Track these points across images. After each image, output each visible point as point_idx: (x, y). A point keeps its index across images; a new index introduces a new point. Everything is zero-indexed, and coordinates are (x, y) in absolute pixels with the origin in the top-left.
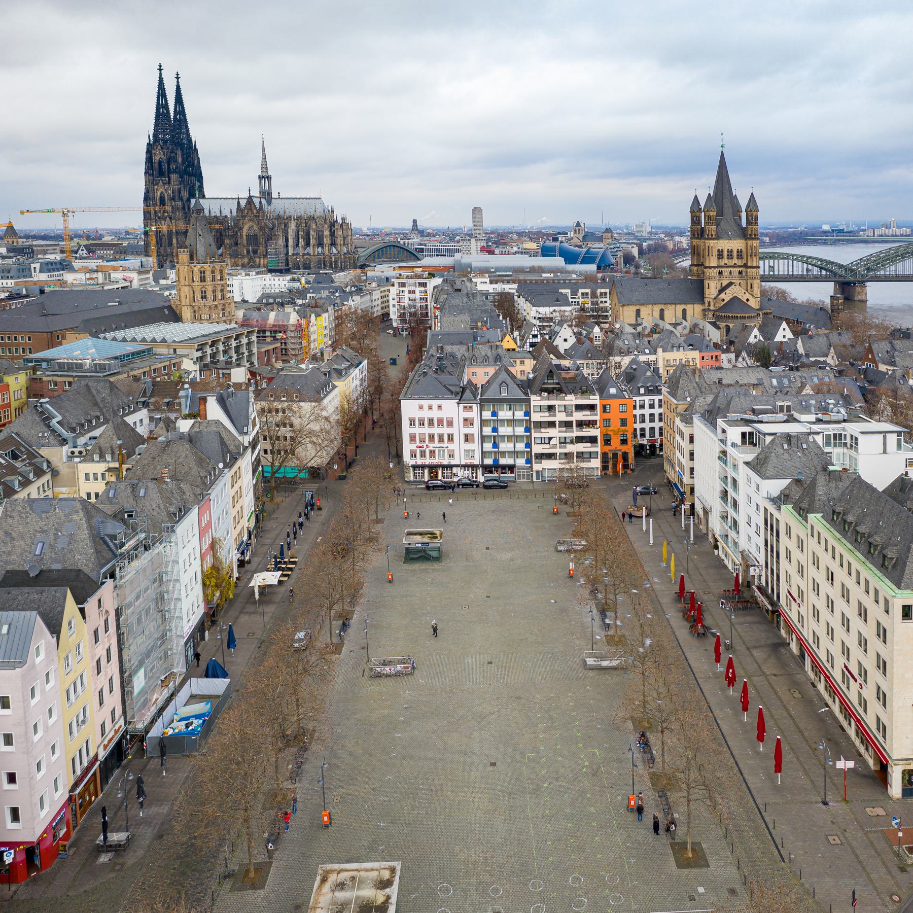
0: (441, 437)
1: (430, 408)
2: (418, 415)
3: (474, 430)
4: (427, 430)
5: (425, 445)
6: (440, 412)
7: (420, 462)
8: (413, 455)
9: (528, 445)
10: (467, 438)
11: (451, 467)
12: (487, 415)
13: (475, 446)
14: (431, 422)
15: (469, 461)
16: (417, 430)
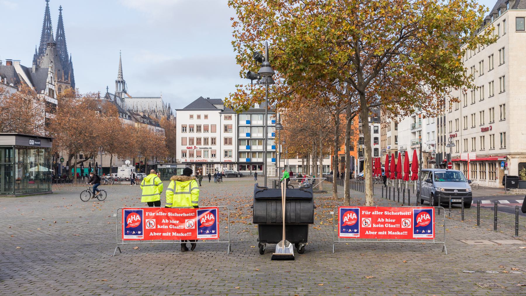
0: (206, 140)
1: (199, 117)
2: (189, 122)
3: (232, 135)
4: (195, 135)
6: (206, 120)
7: (189, 160)
8: (184, 154)
11: (213, 163)
13: (233, 148)
14: (199, 128)
15: (227, 159)
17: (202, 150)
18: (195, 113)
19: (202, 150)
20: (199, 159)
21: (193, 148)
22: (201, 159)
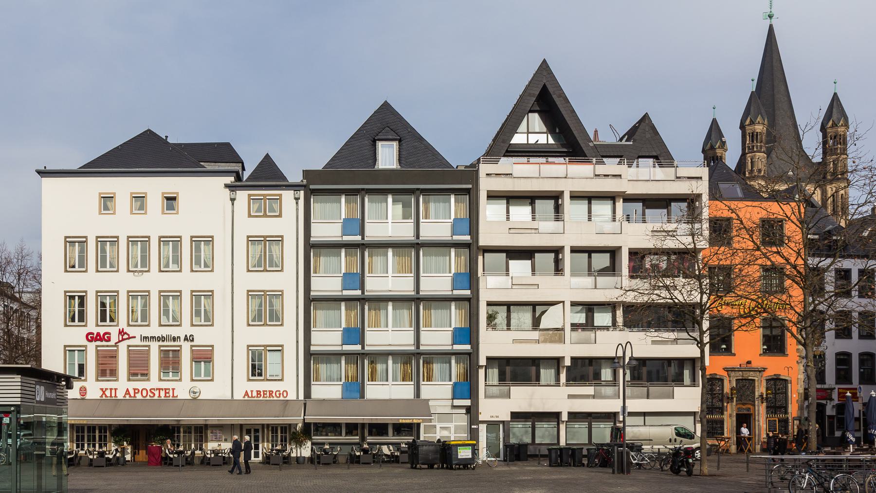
1: (140, 200)
2: (94, 225)
3: (286, 281)
4: (121, 282)
5: (114, 332)
6: (170, 218)
9: (469, 333)
10: (265, 309)
12: (327, 229)
16: (91, 282)
18: (123, 187)
19: (154, 347)
20: (140, 385)
21: (115, 338)
22: (148, 385)
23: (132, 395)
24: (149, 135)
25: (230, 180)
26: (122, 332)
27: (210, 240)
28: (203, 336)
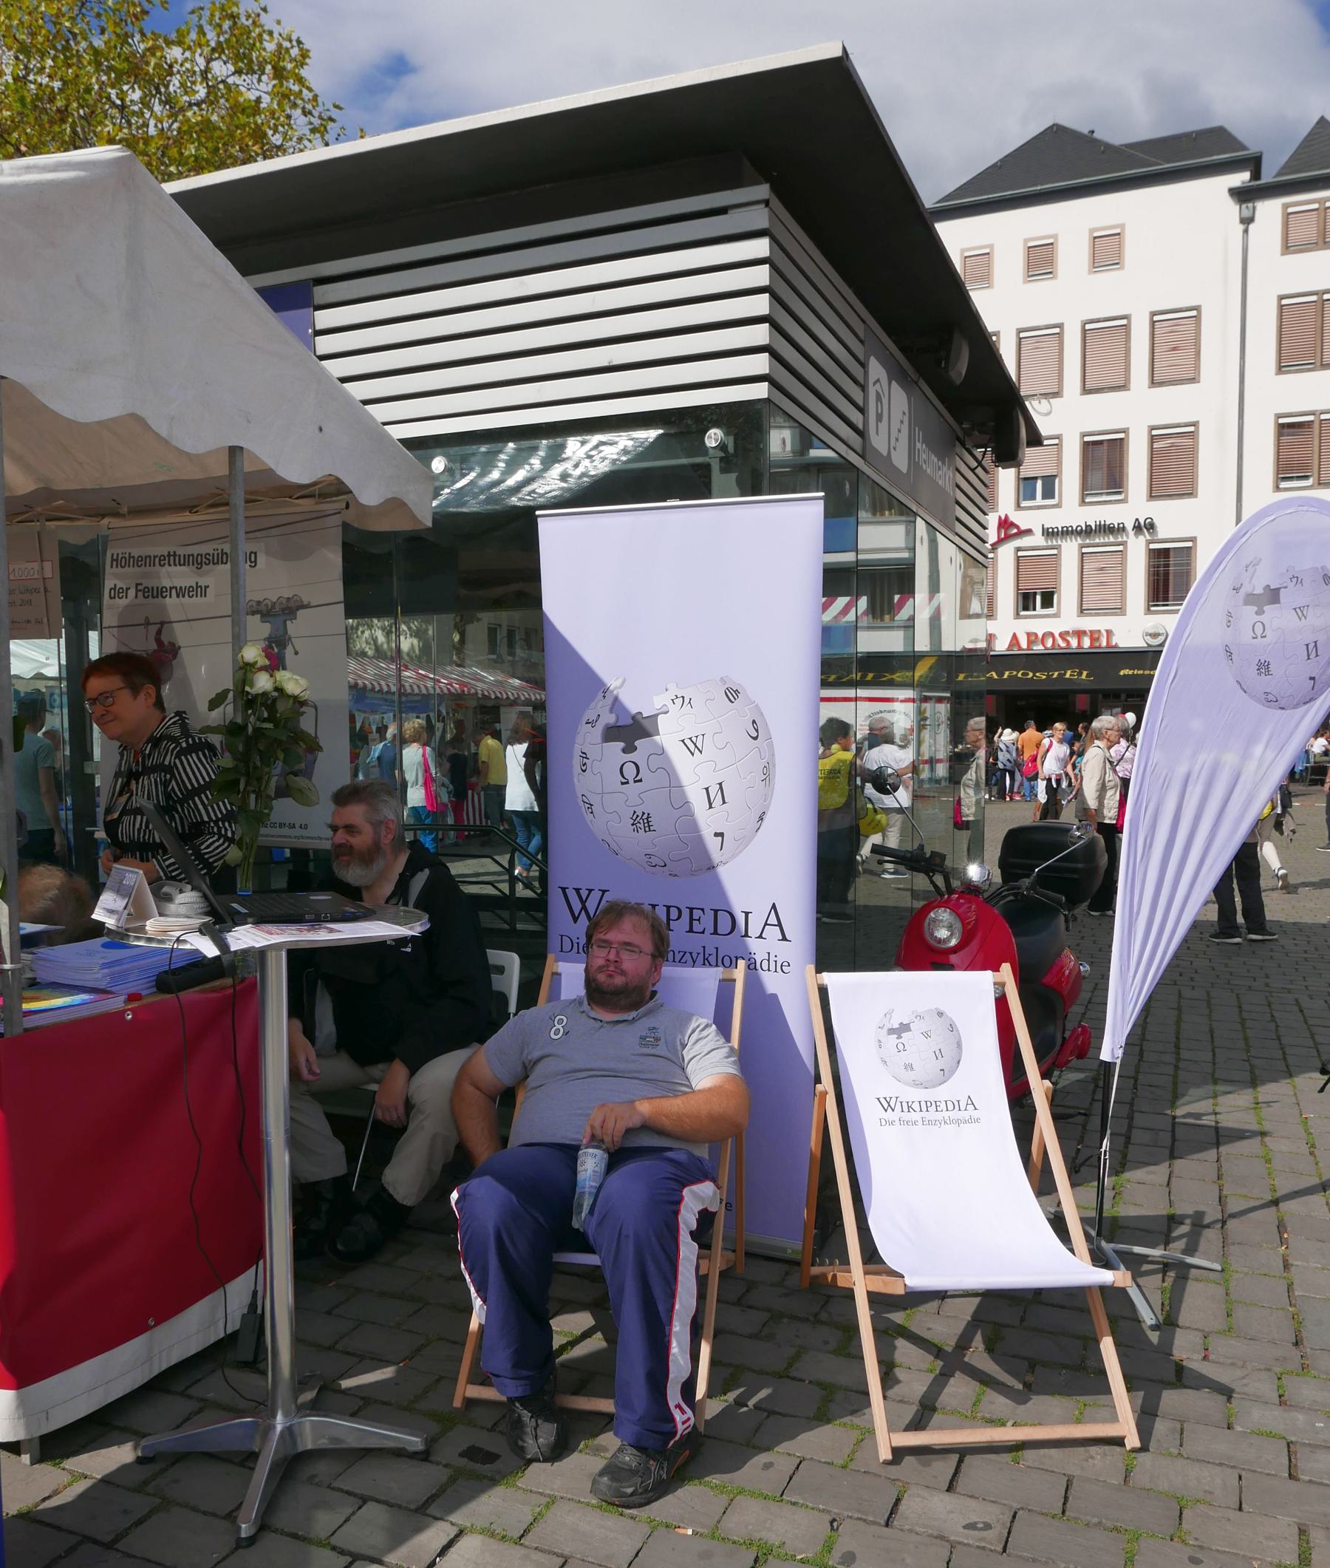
17: (1070, 549)
19: (1070, 549)
22: (1056, 626)
23: (1024, 645)
24: (1056, 134)
25: (1241, 178)
26: (1005, 524)
27: (1195, 314)
28: (1173, 520)
